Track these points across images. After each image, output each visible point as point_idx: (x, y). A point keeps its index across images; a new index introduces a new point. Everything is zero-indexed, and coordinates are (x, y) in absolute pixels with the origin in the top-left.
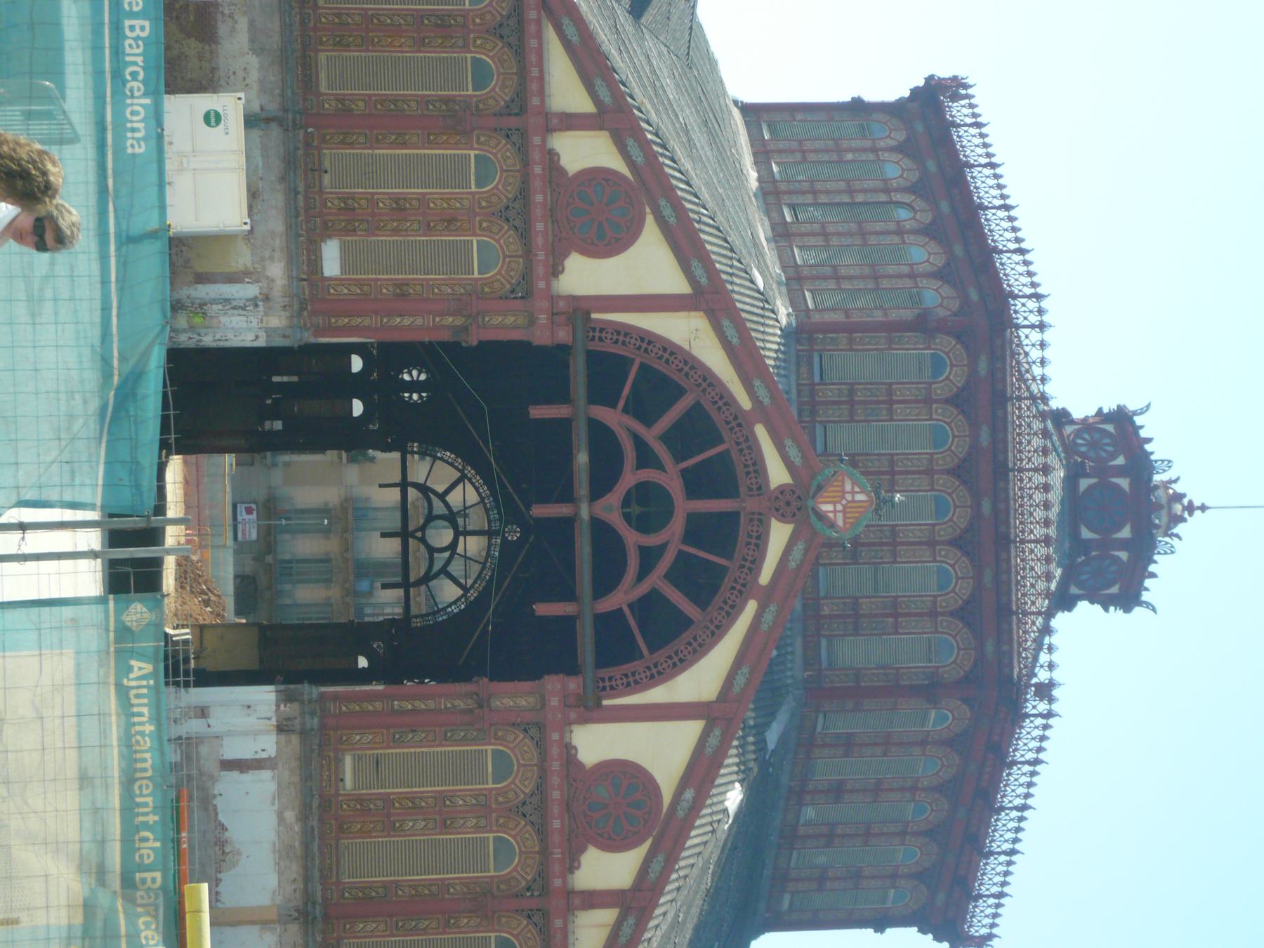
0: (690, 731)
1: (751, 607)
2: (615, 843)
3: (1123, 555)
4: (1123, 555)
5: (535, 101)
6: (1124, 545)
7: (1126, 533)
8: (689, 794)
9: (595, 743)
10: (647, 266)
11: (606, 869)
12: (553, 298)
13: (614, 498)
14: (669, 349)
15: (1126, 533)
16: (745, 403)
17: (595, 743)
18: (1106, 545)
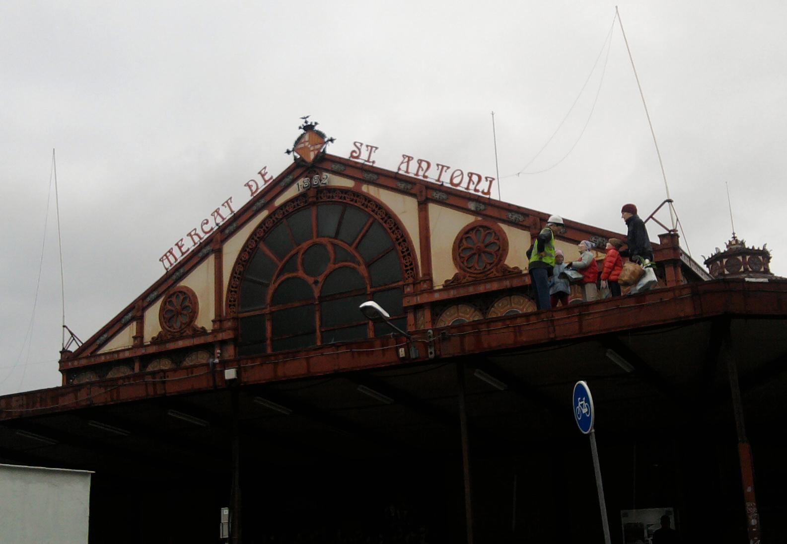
0: (434, 210)
1: (365, 188)
2: (502, 247)
3: (748, 257)
4: (748, 257)
5: (127, 354)
6: (744, 258)
7: (740, 258)
8: (472, 206)
9: (443, 270)
10: (200, 282)
11: (518, 249)
12: (214, 331)
13: (311, 280)
14: (239, 261)
15: (740, 258)
16: (264, 214)
17: (443, 270)
18: (745, 263)
